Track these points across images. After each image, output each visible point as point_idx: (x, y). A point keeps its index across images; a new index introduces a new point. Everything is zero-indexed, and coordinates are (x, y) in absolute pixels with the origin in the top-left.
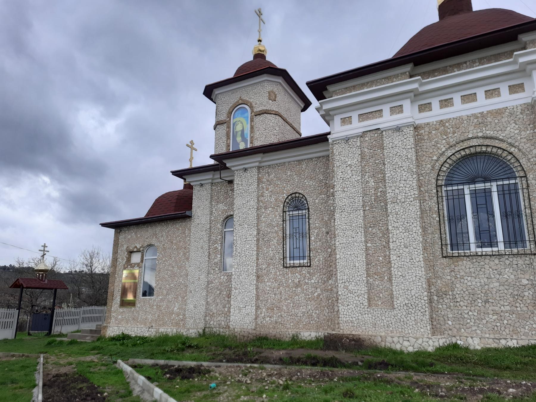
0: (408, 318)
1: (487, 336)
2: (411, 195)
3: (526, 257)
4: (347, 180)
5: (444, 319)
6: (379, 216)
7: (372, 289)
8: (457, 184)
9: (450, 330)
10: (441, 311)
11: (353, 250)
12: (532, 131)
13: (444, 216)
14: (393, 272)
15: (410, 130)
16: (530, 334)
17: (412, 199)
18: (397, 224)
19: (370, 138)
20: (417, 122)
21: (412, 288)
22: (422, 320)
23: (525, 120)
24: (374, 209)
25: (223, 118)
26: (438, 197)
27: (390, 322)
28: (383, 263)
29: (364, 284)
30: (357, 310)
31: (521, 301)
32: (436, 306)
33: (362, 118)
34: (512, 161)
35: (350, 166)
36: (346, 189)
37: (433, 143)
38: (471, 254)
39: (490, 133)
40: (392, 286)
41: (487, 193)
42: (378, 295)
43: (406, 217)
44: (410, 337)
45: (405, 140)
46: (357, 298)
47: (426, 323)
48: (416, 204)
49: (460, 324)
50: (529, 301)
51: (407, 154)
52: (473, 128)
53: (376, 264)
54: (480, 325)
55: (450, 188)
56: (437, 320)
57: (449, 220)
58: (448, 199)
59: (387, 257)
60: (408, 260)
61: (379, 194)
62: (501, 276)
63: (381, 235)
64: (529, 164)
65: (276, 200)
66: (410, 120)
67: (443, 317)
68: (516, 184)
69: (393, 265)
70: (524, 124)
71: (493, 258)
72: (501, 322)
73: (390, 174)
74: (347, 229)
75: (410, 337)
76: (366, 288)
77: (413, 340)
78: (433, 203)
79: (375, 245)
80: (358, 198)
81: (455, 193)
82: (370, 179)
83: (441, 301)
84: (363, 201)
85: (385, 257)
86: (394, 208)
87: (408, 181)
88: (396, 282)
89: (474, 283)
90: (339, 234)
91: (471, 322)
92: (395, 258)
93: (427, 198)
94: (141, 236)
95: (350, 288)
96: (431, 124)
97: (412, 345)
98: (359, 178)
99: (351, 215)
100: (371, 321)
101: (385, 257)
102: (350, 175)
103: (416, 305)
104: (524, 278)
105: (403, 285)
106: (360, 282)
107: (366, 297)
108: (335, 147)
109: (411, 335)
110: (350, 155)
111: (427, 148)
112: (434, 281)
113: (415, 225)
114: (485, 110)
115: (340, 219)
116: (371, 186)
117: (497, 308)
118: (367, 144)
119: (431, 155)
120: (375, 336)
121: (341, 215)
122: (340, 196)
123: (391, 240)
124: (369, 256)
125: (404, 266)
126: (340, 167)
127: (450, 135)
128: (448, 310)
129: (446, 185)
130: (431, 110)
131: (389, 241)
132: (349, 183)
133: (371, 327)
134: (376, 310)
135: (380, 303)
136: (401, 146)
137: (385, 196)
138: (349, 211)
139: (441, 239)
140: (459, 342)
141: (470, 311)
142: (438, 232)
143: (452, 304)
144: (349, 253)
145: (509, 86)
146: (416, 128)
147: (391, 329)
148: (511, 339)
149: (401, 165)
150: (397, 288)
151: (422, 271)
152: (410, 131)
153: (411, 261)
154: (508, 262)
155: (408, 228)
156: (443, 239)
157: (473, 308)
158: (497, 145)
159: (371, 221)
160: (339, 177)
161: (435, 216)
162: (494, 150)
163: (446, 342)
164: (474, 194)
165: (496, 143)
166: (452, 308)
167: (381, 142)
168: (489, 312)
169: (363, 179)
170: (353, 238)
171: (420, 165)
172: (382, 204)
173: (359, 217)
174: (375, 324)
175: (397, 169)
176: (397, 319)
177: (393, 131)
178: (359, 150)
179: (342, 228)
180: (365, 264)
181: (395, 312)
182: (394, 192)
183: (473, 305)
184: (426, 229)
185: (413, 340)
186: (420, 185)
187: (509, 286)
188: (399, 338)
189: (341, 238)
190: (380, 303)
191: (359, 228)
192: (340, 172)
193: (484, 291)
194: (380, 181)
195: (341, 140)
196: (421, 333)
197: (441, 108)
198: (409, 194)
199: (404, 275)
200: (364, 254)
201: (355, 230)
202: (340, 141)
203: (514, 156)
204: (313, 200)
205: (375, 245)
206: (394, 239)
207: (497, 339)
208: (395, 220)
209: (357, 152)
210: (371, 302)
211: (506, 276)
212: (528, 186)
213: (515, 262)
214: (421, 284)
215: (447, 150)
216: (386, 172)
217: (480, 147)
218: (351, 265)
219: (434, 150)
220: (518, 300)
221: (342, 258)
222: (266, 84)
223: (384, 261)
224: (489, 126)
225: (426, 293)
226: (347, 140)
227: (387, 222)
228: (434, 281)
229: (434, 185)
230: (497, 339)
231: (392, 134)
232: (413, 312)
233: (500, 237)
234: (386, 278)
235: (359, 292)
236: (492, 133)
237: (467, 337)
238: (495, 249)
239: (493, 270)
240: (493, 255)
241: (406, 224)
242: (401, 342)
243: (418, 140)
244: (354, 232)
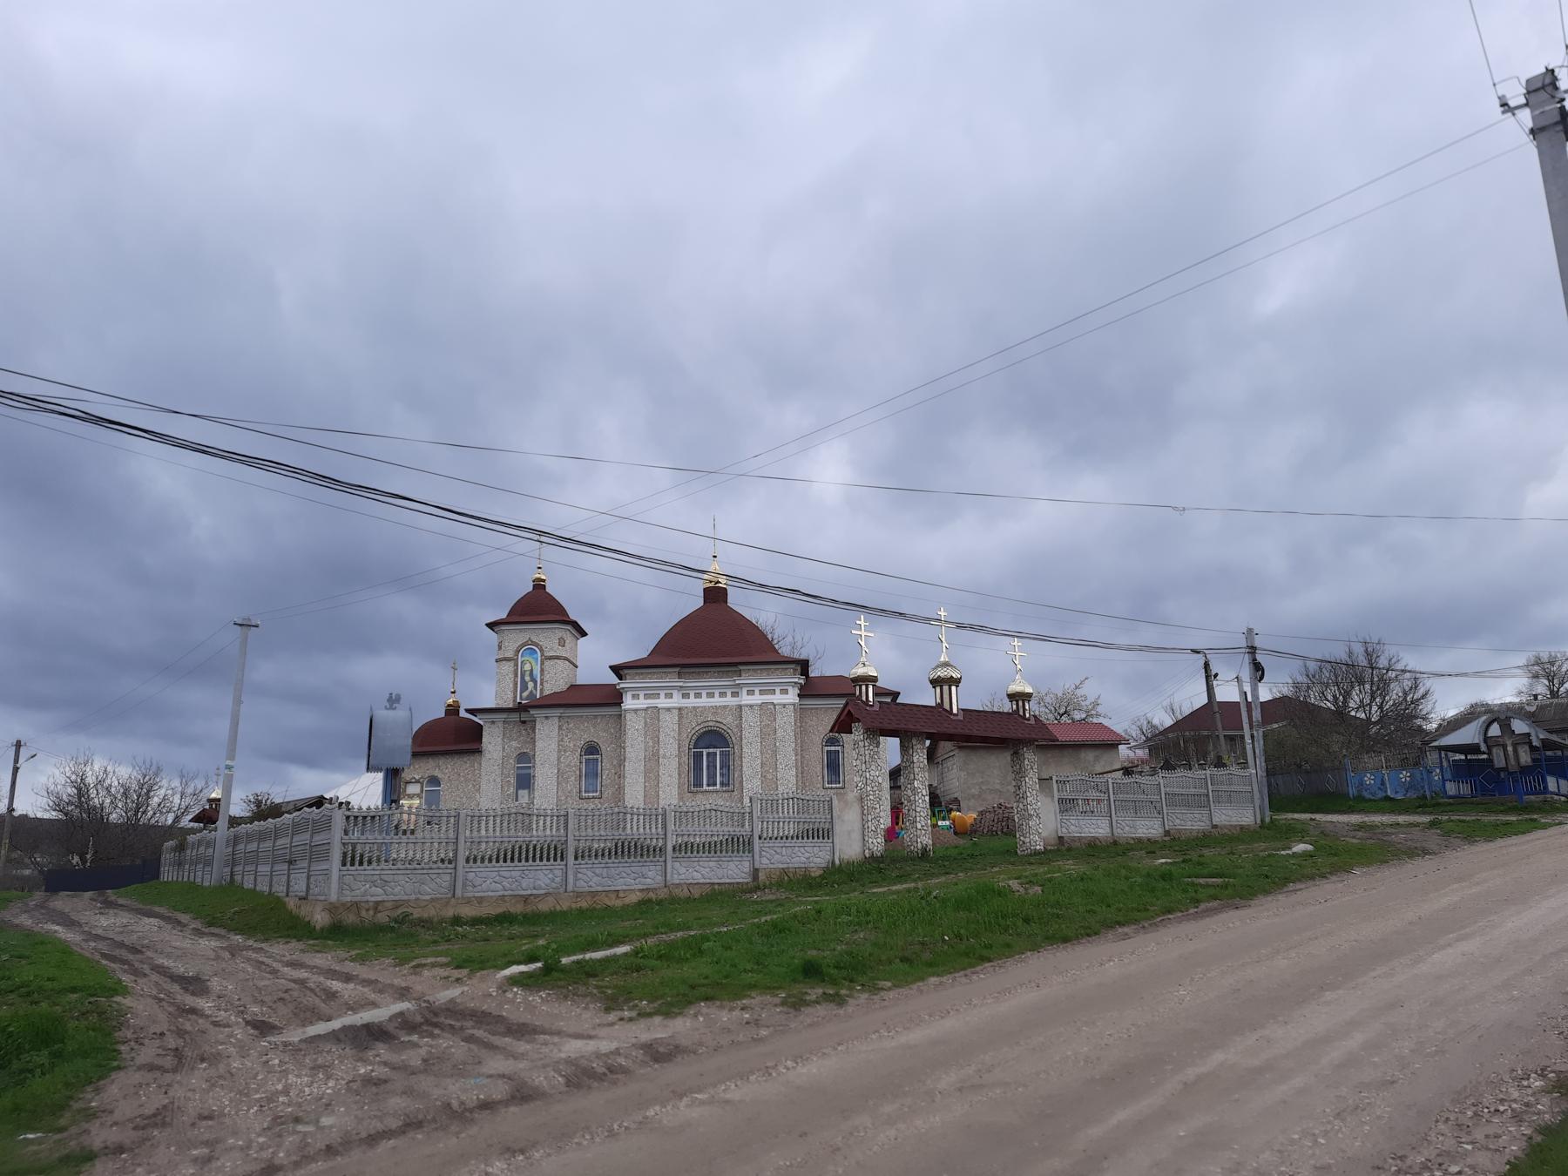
25: (509, 654)
35: (637, 730)
65: (574, 745)
78: (685, 759)
94: (420, 767)
114: (718, 704)
146: (680, 709)
152: (676, 712)
164: (708, 754)
165: (721, 726)
204: (606, 748)
222: (557, 631)
226: (636, 711)
233: (718, 782)
243: (680, 717)
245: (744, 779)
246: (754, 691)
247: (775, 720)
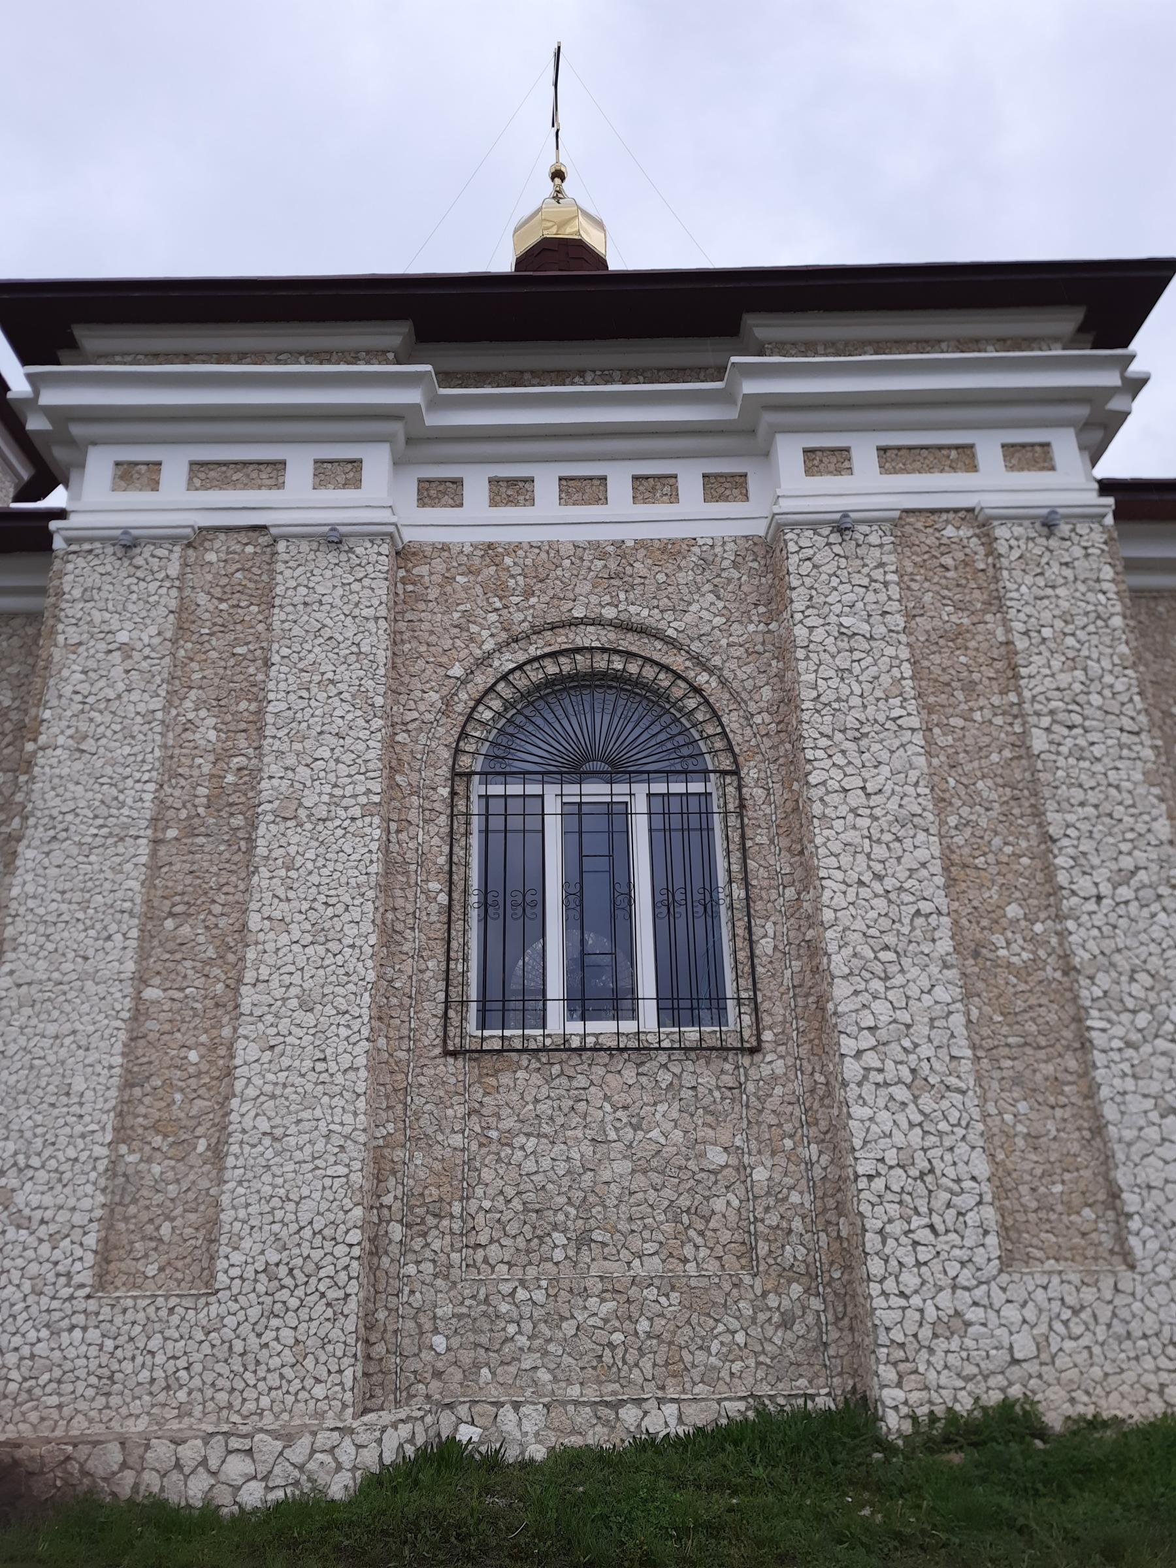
0: (269, 1336)
1: (574, 1391)
2: (355, 796)
3: (726, 1060)
4: (102, 706)
5: (419, 1326)
6: (214, 869)
7: (127, 1200)
8: (524, 776)
9: (438, 1374)
10: (412, 1292)
11: (74, 1016)
12: (762, 627)
13: (466, 892)
14: (234, 1117)
15: (380, 554)
16: (724, 1374)
17: (356, 812)
18: (284, 906)
19: (223, 556)
20: (409, 535)
21: (305, 1192)
22: (325, 1342)
23: (745, 588)
24: (201, 840)
26: (452, 816)
27: (182, 1363)
28: (198, 1075)
29: (93, 1175)
30: (34, 1310)
31: (701, 1233)
32: (393, 1270)
33: (203, 476)
34: (700, 716)
35: (126, 650)
36: (86, 746)
37: (456, 615)
38: (548, 1042)
39: (639, 613)
40: (222, 1182)
41: (618, 814)
42: (150, 1228)
43: (325, 881)
44: (261, 1430)
45: (356, 586)
46: (45, 1249)
47: (339, 1353)
48: (368, 830)
49: (477, 1345)
50: (725, 1236)
51: (360, 636)
52: (588, 587)
53: (168, 1083)
54: (551, 1347)
55: (496, 789)
56: (388, 1335)
57: (485, 905)
58: (487, 831)
59: (222, 1051)
60: (308, 1064)
61: (230, 778)
62: (640, 1134)
63: (211, 953)
64: (748, 732)
66: (384, 516)
67: (415, 1318)
68: (707, 795)
69: (239, 1085)
70: (742, 601)
71: (618, 1062)
72: (627, 1325)
73: (284, 706)
74: (65, 917)
75: (261, 1430)
76: (101, 1199)
77: (268, 1446)
79: (178, 995)
80: (138, 786)
81: (515, 806)
82: (203, 713)
83: (418, 1243)
84: (159, 802)
85: (213, 1048)
86: (283, 842)
87: (349, 740)
88: (240, 1163)
89: (546, 1163)
90: (22, 940)
91: (520, 1332)
92: (253, 1052)
93: (413, 815)
95: (19, 1199)
96: (454, 551)
97: (263, 1470)
98: (156, 704)
99: (93, 858)
100: (93, 1365)
101: (213, 1048)
102: (121, 686)
103: (310, 1267)
104: (715, 1144)
105: (267, 1178)
106: (77, 1166)
107: (91, 1240)
108: (70, 567)
109: (268, 1420)
110: (131, 607)
111: (432, 632)
112: (399, 1154)
113: (356, 914)
114: (628, 534)
115: (40, 871)
116: (203, 742)
117: (615, 1268)
118: (209, 577)
119: (444, 660)
120: (95, 1443)
121: (47, 854)
122: (57, 771)
123: (249, 976)
124: (142, 1042)
125: (290, 1090)
126: (82, 649)
127: (515, 599)
128: (439, 1282)
129: (487, 776)
130: (461, 505)
131: (239, 981)
132: (108, 718)
133: (90, 1392)
134: (129, 1303)
135: (151, 1270)
136: (338, 602)
137: (253, 788)
138: (89, 840)
139: (447, 980)
140: (466, 1433)
141: (522, 1282)
142: (440, 950)
143: (455, 1256)
144: (52, 1029)
145: (704, 476)
146: (403, 555)
147: (182, 1395)
148: (660, 1401)
149: (330, 675)
150: (241, 1190)
151: (355, 1114)
152: (378, 557)
153: (320, 1066)
154: (665, 1078)
155: (327, 925)
156: (456, 980)
157: (532, 1272)
158: (656, 657)
159: (180, 888)
160: (70, 688)
161: (434, 886)
162: (649, 672)
163: (411, 1440)
164: (576, 813)
165: (655, 649)
166: (455, 1273)
167: (265, 577)
168: (589, 1283)
169: (174, 712)
170: (86, 958)
171: (402, 689)
172: (238, 821)
173: (128, 867)
174: (111, 1378)
175: (314, 690)
176: (217, 1342)
177: (315, 546)
178: (174, 593)
179: (42, 911)
180: (115, 1081)
181: (214, 1309)
182: (290, 774)
183: (535, 1258)
184: (397, 937)
185: (268, 1446)
186: (394, 763)
187: (663, 1173)
188: (206, 1444)
189: (24, 956)
190: (151, 1270)
191: (118, 916)
192: (75, 667)
193: (577, 1195)
194: (243, 726)
195: (103, 540)
196: (312, 1403)
197: (493, 503)
198: (349, 790)
199: (278, 1132)
200: (123, 1036)
201: (98, 926)
202: (98, 545)
203: (707, 701)
205: (178, 995)
206: (264, 972)
207: (607, 1404)
208: (281, 892)
209: (163, 602)
210: (112, 1267)
211: (654, 1134)
212: (742, 806)
213: (688, 1080)
214: (343, 1170)
215: (499, 649)
216: (271, 696)
217: (606, 656)
218: (51, 1089)
219: (458, 643)
220: (692, 1233)
221: (9, 1053)
223: (204, 1067)
224: (638, 590)
225: (358, 1212)
227: (247, 896)
228: (399, 1154)
229: (444, 771)
230: (607, 1404)
231: (312, 556)
232: (293, 1303)
234: (202, 1145)
235: (63, 1216)
236: (645, 613)
237: (498, 1405)
238: (628, 1026)
239: (616, 1110)
240: (618, 1049)
241: (321, 908)
242: (213, 1464)
244: (92, 933)
245: (838, 963)
246: (843, 453)
247: (997, 602)
